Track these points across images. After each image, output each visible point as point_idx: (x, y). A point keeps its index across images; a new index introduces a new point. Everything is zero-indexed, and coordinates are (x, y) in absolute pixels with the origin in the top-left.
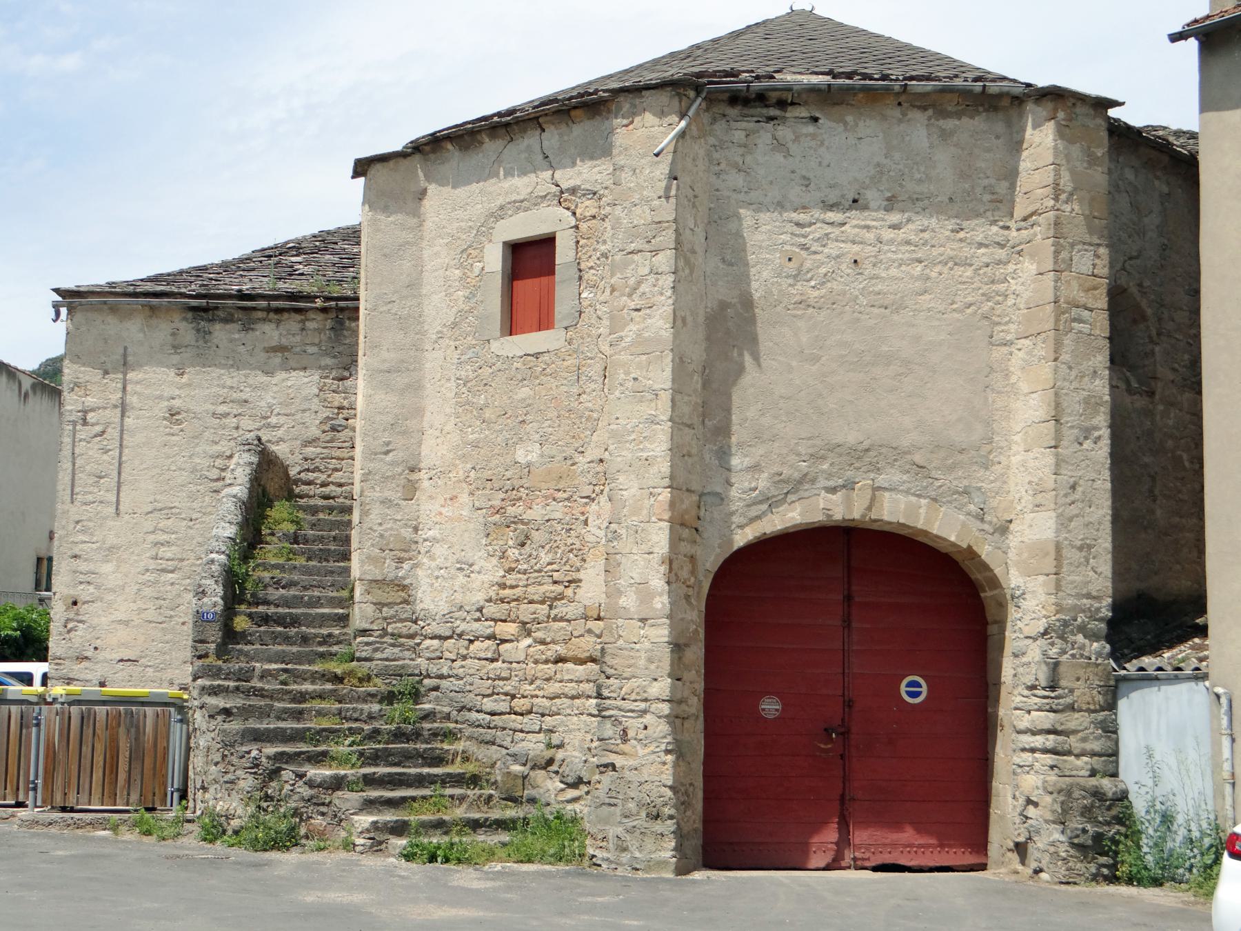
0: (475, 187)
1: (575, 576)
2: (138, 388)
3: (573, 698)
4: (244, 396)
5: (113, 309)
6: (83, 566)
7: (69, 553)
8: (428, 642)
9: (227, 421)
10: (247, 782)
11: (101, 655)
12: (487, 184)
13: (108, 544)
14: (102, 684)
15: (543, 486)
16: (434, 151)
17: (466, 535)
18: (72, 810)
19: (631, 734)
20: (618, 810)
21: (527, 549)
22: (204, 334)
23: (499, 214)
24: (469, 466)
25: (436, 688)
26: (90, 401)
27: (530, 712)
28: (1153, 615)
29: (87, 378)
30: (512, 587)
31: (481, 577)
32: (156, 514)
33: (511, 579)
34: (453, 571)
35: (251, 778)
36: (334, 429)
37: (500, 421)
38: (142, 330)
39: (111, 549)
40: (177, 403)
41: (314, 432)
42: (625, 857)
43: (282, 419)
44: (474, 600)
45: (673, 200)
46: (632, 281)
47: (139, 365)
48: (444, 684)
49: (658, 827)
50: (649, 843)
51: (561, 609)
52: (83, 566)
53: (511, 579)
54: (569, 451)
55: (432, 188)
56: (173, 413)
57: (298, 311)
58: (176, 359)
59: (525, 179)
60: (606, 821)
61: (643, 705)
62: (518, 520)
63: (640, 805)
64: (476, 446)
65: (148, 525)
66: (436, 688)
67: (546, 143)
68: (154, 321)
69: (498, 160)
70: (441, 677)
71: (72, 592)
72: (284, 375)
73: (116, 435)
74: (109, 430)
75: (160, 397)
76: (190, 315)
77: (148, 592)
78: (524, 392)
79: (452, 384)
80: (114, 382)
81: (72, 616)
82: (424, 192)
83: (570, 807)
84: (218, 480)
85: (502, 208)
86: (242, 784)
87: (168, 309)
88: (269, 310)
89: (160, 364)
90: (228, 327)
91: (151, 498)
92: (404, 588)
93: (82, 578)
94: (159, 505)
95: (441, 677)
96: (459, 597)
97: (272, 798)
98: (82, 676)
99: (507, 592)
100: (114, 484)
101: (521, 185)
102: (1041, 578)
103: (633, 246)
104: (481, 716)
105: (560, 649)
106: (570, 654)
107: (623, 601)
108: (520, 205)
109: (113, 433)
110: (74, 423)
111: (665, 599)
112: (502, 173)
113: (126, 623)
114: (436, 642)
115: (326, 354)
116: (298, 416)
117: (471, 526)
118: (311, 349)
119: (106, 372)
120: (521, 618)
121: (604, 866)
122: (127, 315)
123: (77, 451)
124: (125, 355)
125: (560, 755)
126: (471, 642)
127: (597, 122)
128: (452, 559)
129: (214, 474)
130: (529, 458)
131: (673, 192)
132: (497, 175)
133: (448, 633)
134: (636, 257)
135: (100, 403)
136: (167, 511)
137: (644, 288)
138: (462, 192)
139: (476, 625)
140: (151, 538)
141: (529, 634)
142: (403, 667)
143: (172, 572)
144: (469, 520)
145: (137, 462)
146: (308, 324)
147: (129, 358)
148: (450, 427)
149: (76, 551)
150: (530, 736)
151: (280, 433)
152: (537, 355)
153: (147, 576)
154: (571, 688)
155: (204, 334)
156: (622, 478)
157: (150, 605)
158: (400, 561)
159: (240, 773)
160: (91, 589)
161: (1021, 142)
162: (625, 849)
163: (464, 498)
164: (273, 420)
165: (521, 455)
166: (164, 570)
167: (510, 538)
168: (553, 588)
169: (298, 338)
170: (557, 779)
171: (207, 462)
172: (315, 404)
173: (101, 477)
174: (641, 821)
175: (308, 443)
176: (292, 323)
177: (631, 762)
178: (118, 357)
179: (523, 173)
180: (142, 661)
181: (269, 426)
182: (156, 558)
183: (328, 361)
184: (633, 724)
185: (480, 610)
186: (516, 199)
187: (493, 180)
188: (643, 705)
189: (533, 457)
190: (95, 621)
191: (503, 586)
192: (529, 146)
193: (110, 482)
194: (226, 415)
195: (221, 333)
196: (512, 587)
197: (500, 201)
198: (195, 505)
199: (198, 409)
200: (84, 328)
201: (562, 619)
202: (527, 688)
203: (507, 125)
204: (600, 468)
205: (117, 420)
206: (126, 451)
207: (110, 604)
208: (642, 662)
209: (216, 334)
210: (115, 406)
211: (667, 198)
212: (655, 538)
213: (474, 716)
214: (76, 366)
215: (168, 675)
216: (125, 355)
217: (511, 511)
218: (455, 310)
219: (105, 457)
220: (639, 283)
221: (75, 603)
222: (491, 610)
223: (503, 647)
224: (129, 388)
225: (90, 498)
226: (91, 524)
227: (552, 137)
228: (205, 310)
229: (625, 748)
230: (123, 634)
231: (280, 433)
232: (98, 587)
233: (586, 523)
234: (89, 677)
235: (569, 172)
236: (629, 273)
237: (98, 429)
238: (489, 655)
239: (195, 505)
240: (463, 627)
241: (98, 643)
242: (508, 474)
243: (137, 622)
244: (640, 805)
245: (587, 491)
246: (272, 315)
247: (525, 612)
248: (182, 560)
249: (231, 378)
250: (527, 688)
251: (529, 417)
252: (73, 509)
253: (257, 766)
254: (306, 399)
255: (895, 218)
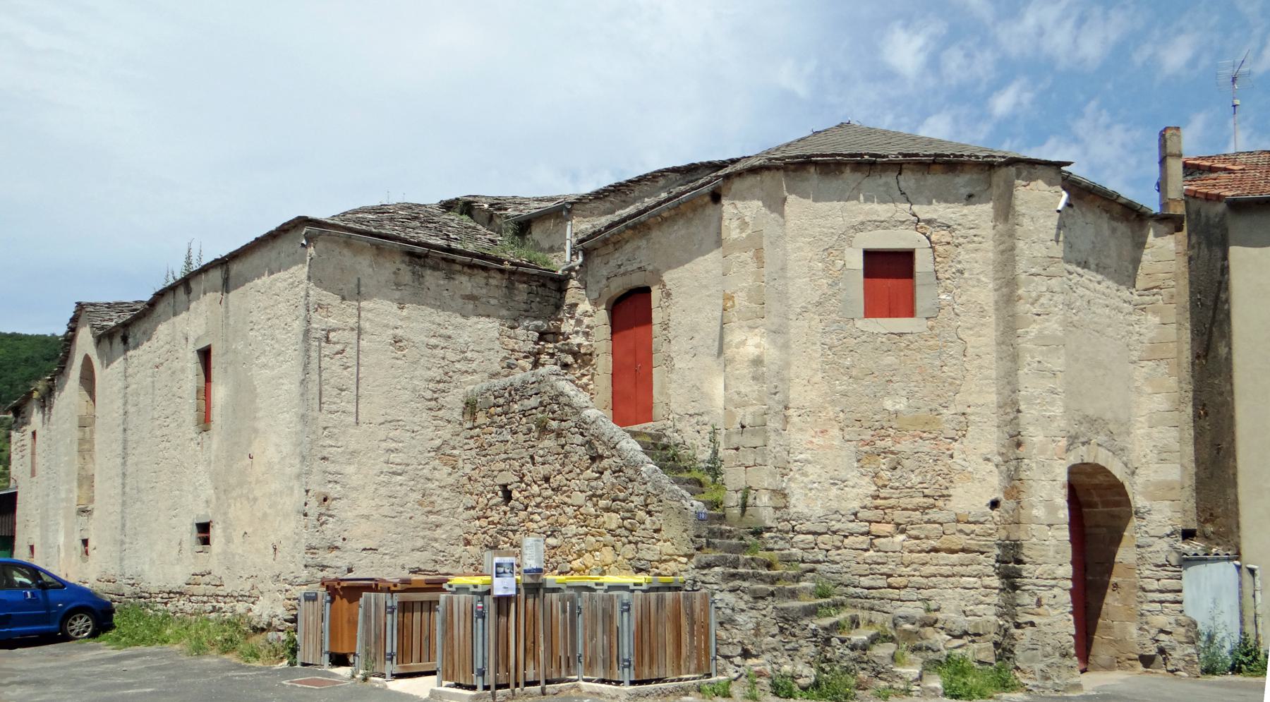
0: (837, 205)
1: (945, 492)
2: (370, 315)
3: (948, 576)
4: (449, 332)
5: (348, 243)
6: (331, 467)
7: (320, 455)
8: (802, 537)
9: (436, 352)
10: (809, 650)
11: (350, 545)
12: (848, 204)
13: (351, 448)
14: (350, 570)
15: (910, 427)
16: (794, 171)
17: (839, 460)
18: (648, 682)
19: (1044, 601)
20: (1039, 653)
21: (898, 472)
22: (419, 277)
23: (860, 227)
24: (838, 409)
25: (812, 571)
26: (332, 322)
27: (906, 587)
28: (1213, 520)
29: (329, 301)
30: (885, 498)
31: (855, 490)
32: (388, 425)
33: (884, 493)
34: (827, 486)
35: (812, 645)
36: (509, 367)
37: (868, 378)
38: (371, 266)
39: (353, 453)
40: (399, 332)
41: (497, 367)
42: (1049, 683)
43: (475, 355)
44: (851, 506)
45: (1061, 244)
46: (1034, 294)
47: (368, 297)
48: (818, 566)
49: (1068, 662)
50: (1064, 674)
51: (933, 514)
52: (331, 467)
53: (884, 493)
54: (935, 405)
55: (792, 198)
56: (397, 340)
57: (485, 268)
58: (397, 295)
59: (884, 206)
60: (1032, 660)
61: (1053, 582)
62: (886, 452)
63: (1054, 648)
64: (845, 395)
65: (382, 433)
66: (812, 571)
67: (902, 184)
68: (381, 260)
69: (858, 188)
70: (818, 562)
71: (323, 490)
72: (474, 319)
73: (354, 354)
74: (348, 349)
75: (387, 326)
76: (407, 259)
77: (383, 491)
78: (890, 359)
79: (818, 347)
80: (350, 307)
81: (323, 511)
82: (785, 199)
83: (959, 651)
84: (431, 400)
85: (863, 223)
86: (805, 650)
87: (391, 251)
88: (464, 264)
89: (386, 297)
90: (436, 273)
91: (383, 412)
92: (785, 496)
93: (330, 477)
94: (389, 418)
95: (818, 562)
96: (835, 505)
97: (829, 660)
98: (333, 564)
99: (879, 502)
100: (353, 397)
101: (882, 210)
102: (1168, 503)
103: (1033, 270)
104: (858, 590)
105: (934, 543)
106: (944, 546)
107: (1035, 512)
108: (879, 224)
109: (350, 352)
110: (319, 340)
111: (1067, 511)
112: (862, 198)
113: (367, 517)
114: (810, 537)
115: (502, 306)
116: (486, 353)
117: (843, 453)
118: (493, 301)
119: (343, 299)
120: (897, 520)
121: (1035, 690)
122: (358, 251)
123: (323, 365)
124: (359, 286)
125: (938, 615)
126: (846, 537)
127: (949, 177)
128: (825, 476)
129: (429, 394)
130: (897, 407)
131: (1061, 238)
132: (858, 199)
133: (823, 530)
134: (1035, 278)
135: (340, 325)
136: (395, 422)
137: (1042, 300)
138: (823, 206)
139: (851, 525)
140: (384, 445)
141: (903, 531)
142: (790, 555)
143: (400, 474)
144: (841, 448)
145: (371, 379)
146: (491, 281)
147: (362, 289)
148: (818, 378)
149: (325, 454)
150: (908, 604)
151: (474, 365)
152: (900, 335)
153: (383, 478)
154: (946, 570)
155: (419, 277)
156: (1031, 429)
157: (385, 502)
158: (783, 475)
159: (802, 642)
160: (338, 487)
161: (1144, 243)
162: (1048, 678)
163: (835, 432)
164: (469, 355)
165: (888, 404)
166: (394, 473)
167: (884, 463)
168: (925, 500)
169: (484, 291)
170: (943, 633)
171: (423, 384)
172: (497, 345)
173: (342, 390)
174: (1056, 659)
175: (494, 375)
176: (480, 277)
177: (1045, 620)
178: (353, 285)
179: (883, 201)
180: (381, 550)
181: (466, 359)
182: (387, 463)
183: (504, 312)
184: (1046, 595)
185: (855, 514)
186: (884, 220)
187: (855, 202)
188: (1053, 582)
189: (902, 405)
190: (343, 515)
191: (876, 497)
192: (886, 184)
193: (349, 395)
194: (435, 347)
195: (432, 279)
196: (885, 498)
197: (861, 218)
198: (416, 419)
199: (416, 339)
200: (324, 256)
201: (935, 522)
202: (903, 570)
203: (874, 163)
204: (962, 418)
205: (355, 341)
206: (362, 369)
207: (354, 501)
208: (1051, 553)
209: (427, 278)
210: (352, 329)
211: (1057, 241)
212: (1058, 471)
213: (851, 590)
214: (319, 290)
215: (400, 561)
216: (359, 286)
217: (879, 444)
218: (819, 292)
219: (345, 373)
220: (1039, 296)
221: (325, 500)
222: (863, 514)
223: (876, 541)
224: (362, 314)
225: (334, 407)
226: (336, 431)
227: (908, 180)
228: (419, 256)
229: (1040, 610)
230: (365, 527)
231: (474, 365)
232: (343, 486)
233: (951, 456)
234: (339, 564)
235: (925, 208)
236: (1031, 288)
237: (339, 347)
238: (865, 547)
239: (416, 419)
240: (837, 526)
241: (346, 535)
242: (877, 417)
243: (376, 516)
244: (1054, 648)
245: (952, 434)
246: (466, 269)
247: (899, 516)
248: (408, 465)
249: (441, 317)
250: (903, 570)
251: (894, 378)
252: (321, 417)
253: (815, 636)
254: (491, 341)
255: (1099, 277)
